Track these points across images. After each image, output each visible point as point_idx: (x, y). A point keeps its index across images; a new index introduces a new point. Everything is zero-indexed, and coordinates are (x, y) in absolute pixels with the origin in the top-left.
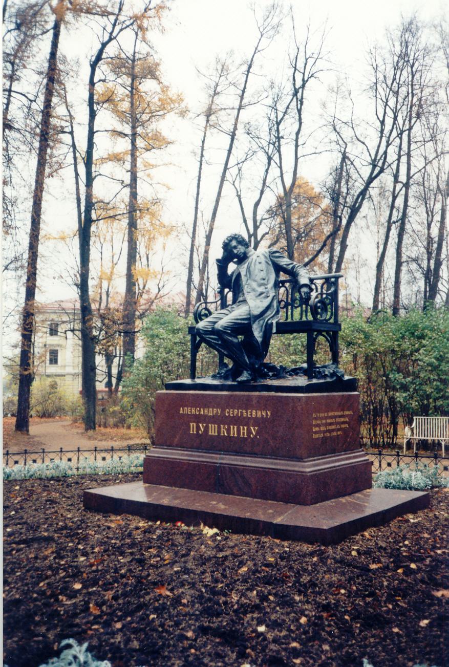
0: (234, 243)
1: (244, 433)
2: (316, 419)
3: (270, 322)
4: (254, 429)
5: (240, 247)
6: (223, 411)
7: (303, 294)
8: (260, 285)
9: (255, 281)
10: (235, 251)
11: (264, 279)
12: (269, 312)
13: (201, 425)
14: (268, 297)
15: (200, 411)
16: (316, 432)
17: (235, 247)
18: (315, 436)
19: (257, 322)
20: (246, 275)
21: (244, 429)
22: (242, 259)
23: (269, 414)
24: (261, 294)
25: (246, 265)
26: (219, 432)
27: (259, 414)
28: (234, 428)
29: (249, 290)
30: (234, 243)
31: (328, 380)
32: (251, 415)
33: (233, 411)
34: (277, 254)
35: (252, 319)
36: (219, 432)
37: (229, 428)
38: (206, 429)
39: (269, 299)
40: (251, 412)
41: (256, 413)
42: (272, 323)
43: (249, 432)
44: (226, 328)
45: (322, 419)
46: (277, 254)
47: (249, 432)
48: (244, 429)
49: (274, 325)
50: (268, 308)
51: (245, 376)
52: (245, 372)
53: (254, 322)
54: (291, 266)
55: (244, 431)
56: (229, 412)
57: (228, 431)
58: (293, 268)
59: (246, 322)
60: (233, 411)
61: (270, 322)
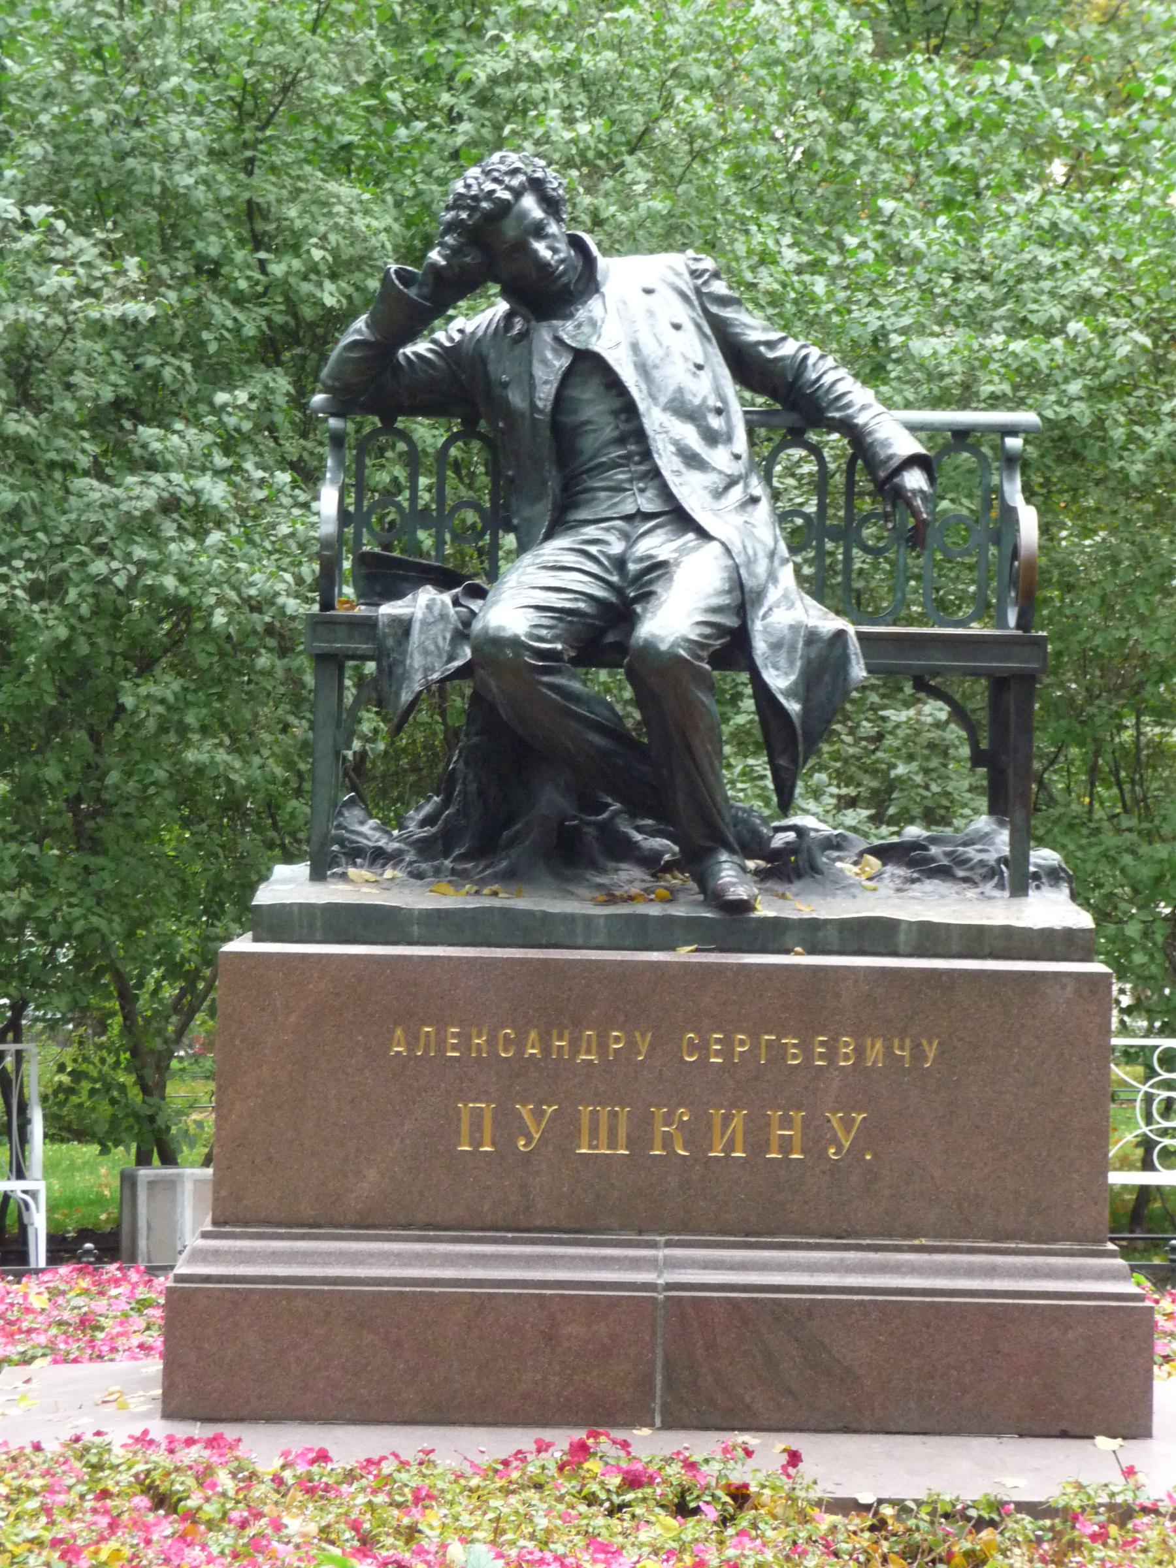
10: (541, 248)
13: (525, 1111)
15: (520, 1043)
17: (538, 231)
22: (548, 294)
23: (931, 1051)
26: (639, 1140)
27: (875, 1051)
28: (727, 1119)
32: (831, 1054)
33: (728, 1042)
36: (639, 1140)
38: (564, 1131)
52: (724, 856)
55: (786, 1131)
56: (703, 1048)
57: (697, 1135)
60: (728, 1042)
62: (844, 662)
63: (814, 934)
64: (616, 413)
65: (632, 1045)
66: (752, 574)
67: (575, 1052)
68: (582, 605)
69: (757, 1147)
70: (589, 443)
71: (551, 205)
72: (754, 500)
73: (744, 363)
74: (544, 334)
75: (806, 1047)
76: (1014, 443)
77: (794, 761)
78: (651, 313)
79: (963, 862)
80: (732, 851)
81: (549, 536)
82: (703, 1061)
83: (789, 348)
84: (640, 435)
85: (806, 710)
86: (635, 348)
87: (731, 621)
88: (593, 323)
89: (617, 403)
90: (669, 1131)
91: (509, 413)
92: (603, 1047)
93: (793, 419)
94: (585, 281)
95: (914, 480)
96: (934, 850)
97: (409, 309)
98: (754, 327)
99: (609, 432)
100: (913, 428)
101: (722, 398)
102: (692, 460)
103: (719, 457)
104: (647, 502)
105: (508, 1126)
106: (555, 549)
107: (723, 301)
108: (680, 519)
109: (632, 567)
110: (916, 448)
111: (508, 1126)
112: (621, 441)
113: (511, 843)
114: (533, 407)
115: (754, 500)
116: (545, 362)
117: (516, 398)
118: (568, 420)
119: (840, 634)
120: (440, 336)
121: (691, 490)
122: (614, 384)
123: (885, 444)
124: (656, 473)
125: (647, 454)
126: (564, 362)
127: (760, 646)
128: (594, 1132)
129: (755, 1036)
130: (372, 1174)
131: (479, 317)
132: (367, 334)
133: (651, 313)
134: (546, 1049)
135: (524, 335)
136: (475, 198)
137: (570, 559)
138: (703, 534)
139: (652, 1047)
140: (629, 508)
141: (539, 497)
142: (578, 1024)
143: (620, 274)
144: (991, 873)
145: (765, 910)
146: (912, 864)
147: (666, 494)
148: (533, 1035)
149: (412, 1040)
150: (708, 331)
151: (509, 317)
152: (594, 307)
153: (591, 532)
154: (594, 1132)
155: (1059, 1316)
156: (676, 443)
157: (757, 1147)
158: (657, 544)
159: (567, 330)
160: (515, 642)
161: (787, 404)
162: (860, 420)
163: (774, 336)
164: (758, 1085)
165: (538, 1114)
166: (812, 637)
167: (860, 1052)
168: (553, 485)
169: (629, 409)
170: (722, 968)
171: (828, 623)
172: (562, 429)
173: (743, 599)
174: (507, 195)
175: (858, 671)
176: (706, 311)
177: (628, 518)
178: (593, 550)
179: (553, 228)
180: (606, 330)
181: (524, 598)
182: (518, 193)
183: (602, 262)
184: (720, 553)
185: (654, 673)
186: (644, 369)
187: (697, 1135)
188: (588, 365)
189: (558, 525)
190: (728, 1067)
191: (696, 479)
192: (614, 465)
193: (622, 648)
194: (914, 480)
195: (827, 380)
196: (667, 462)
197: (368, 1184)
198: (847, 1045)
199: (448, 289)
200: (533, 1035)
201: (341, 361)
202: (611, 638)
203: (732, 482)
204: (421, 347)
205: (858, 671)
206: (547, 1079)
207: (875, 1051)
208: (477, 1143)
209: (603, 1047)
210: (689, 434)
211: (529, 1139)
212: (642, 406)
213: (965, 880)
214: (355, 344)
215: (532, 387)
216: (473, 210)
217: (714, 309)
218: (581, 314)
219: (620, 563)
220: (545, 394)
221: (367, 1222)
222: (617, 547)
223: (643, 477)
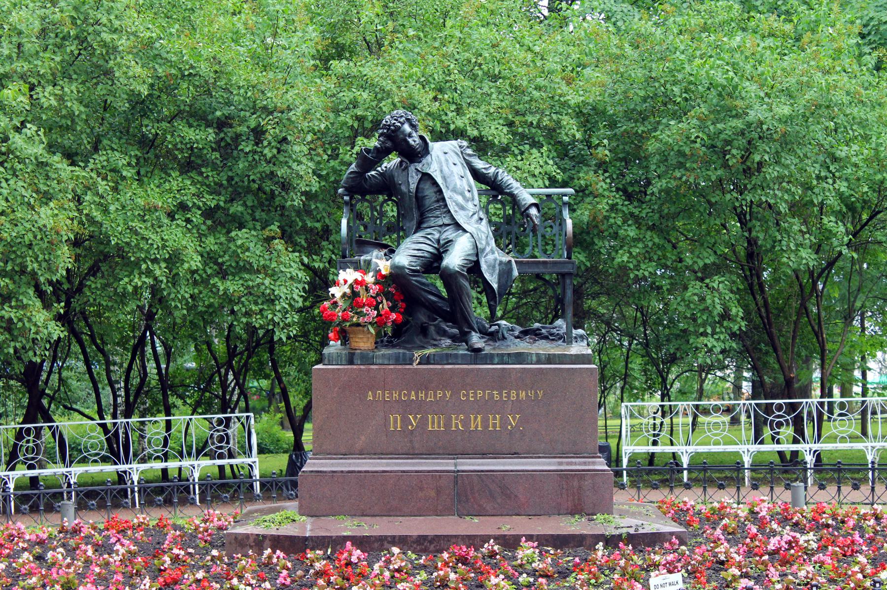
0: (407, 128)
1: (494, 425)
6: (455, 393)
10: (410, 140)
15: (409, 395)
17: (410, 135)
22: (413, 155)
23: (540, 394)
26: (448, 425)
27: (523, 395)
28: (476, 418)
30: (407, 128)
32: (508, 396)
33: (475, 394)
36: (448, 425)
37: (468, 418)
38: (423, 422)
40: (509, 394)
41: (518, 395)
43: (504, 422)
47: (504, 422)
48: (494, 418)
52: (473, 333)
55: (495, 421)
56: (467, 395)
57: (466, 423)
60: (475, 394)
62: (510, 270)
63: (503, 359)
64: (435, 193)
65: (445, 395)
66: (481, 243)
68: (426, 255)
70: (427, 202)
71: (413, 126)
72: (481, 219)
73: (477, 175)
74: (412, 168)
75: (501, 394)
76: (566, 199)
77: (496, 302)
78: (447, 160)
79: (552, 334)
80: (476, 332)
81: (414, 233)
82: (468, 399)
83: (492, 170)
84: (444, 199)
85: (499, 287)
86: (441, 171)
87: (475, 259)
88: (428, 164)
89: (436, 189)
90: (457, 423)
91: (403, 194)
92: (435, 396)
93: (494, 193)
94: (426, 151)
95: (533, 211)
96: (543, 331)
97: (369, 160)
98: (479, 164)
99: (434, 199)
100: (532, 195)
101: (470, 186)
102: (462, 208)
103: (470, 205)
104: (447, 221)
105: (405, 421)
106: (418, 236)
107: (469, 155)
108: (458, 226)
109: (442, 242)
110: (533, 201)
111: (405, 421)
112: (438, 201)
113: (406, 331)
114: (410, 192)
115: (481, 219)
116: (412, 177)
117: (403, 188)
118: (420, 195)
119: (510, 261)
120: (379, 169)
121: (461, 218)
122: (435, 183)
123: (524, 199)
124: (449, 211)
125: (446, 206)
126: (420, 176)
127: (484, 267)
128: (433, 423)
130: (363, 438)
131: (392, 161)
132: (356, 169)
133: (447, 160)
134: (417, 397)
135: (406, 168)
136: (389, 126)
137: (422, 240)
138: (465, 231)
139: (451, 395)
140: (440, 223)
141: (412, 220)
142: (427, 389)
143: (436, 148)
144: (561, 338)
145: (488, 350)
146: (536, 335)
147: (453, 219)
148: (413, 393)
149: (374, 396)
151: (401, 162)
152: (429, 157)
153: (429, 230)
154: (433, 423)
155: (581, 475)
156: (455, 202)
158: (450, 234)
159: (419, 166)
160: (403, 268)
161: (493, 188)
162: (515, 192)
163: (487, 166)
164: (485, 407)
165: (415, 418)
166: (501, 263)
167: (518, 395)
168: (416, 215)
169: (440, 191)
170: (473, 370)
171: (505, 258)
172: (419, 198)
173: (477, 252)
174: (399, 124)
175: (516, 273)
177: (440, 226)
178: (429, 236)
179: (414, 134)
180: (432, 167)
181: (406, 255)
182: (402, 124)
183: (430, 144)
184: (470, 239)
185: (449, 277)
186: (444, 178)
187: (466, 423)
188: (427, 177)
189: (419, 228)
190: (476, 401)
191: (462, 212)
192: (436, 209)
193: (439, 267)
194: (533, 211)
195: (504, 180)
196: (452, 207)
197: (361, 442)
198: (513, 393)
199: (381, 153)
200: (413, 393)
201: (347, 178)
202: (436, 265)
203: (474, 214)
204: (373, 173)
205: (516, 273)
206: (420, 407)
207: (523, 395)
209: (435, 396)
210: (460, 199)
211: (413, 425)
212: (444, 191)
213: (553, 340)
214: (351, 173)
215: (409, 185)
216: (388, 129)
217: (467, 158)
218: (424, 161)
219: (438, 241)
220: (413, 187)
221: (362, 453)
222: (437, 236)
223: (445, 212)
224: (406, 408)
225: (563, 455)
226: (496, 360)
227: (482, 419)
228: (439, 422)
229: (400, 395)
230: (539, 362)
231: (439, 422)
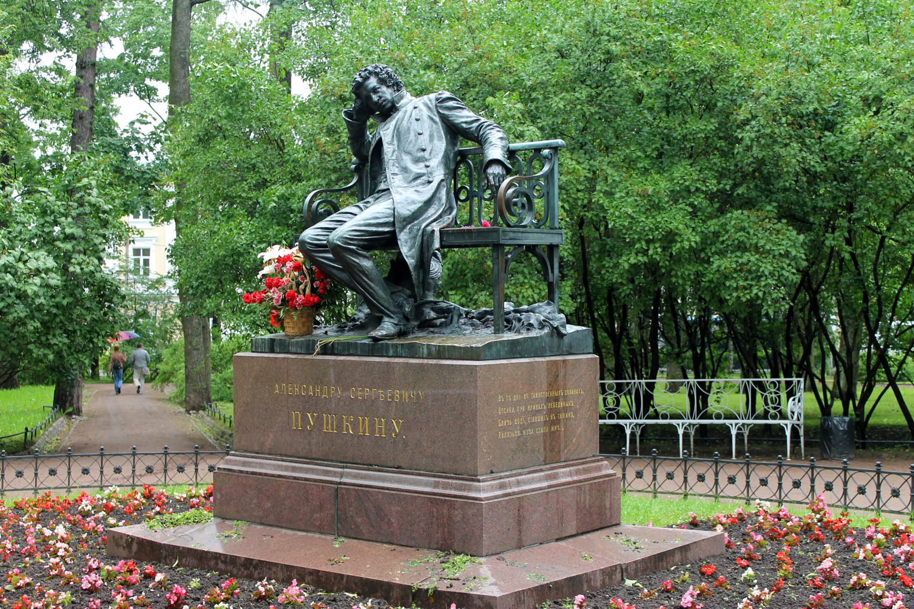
0: (373, 82)
2: (503, 404)
3: (429, 228)
4: (398, 423)
5: (384, 88)
7: (491, 178)
8: (417, 161)
9: (409, 153)
10: (375, 98)
11: (424, 150)
12: (431, 211)
14: (430, 182)
15: (307, 390)
16: (504, 429)
17: (375, 90)
18: (502, 435)
19: (407, 230)
20: (391, 143)
21: (380, 423)
24: (418, 177)
25: (394, 122)
28: (364, 420)
29: (396, 171)
30: (373, 82)
31: (534, 333)
33: (363, 391)
34: (451, 103)
35: (397, 225)
36: (339, 427)
39: (434, 185)
42: (433, 231)
44: (347, 240)
45: (514, 405)
46: (451, 103)
49: (437, 234)
50: (428, 203)
51: (387, 327)
52: (386, 319)
53: (402, 230)
54: (475, 125)
57: (355, 426)
58: (480, 127)
59: (386, 229)
61: (429, 228)
67: (322, 394)
69: (372, 431)
129: (371, 389)
130: (271, 436)
134: (314, 393)
150: (437, 119)
157: (372, 431)
170: (360, 363)
176: (438, 112)
207: (406, 394)
208: (297, 426)
224: (309, 404)
225: (442, 473)
226: (391, 353)
227: (370, 421)
228: (332, 424)
229: (300, 390)
230: (430, 356)
231: (332, 424)
